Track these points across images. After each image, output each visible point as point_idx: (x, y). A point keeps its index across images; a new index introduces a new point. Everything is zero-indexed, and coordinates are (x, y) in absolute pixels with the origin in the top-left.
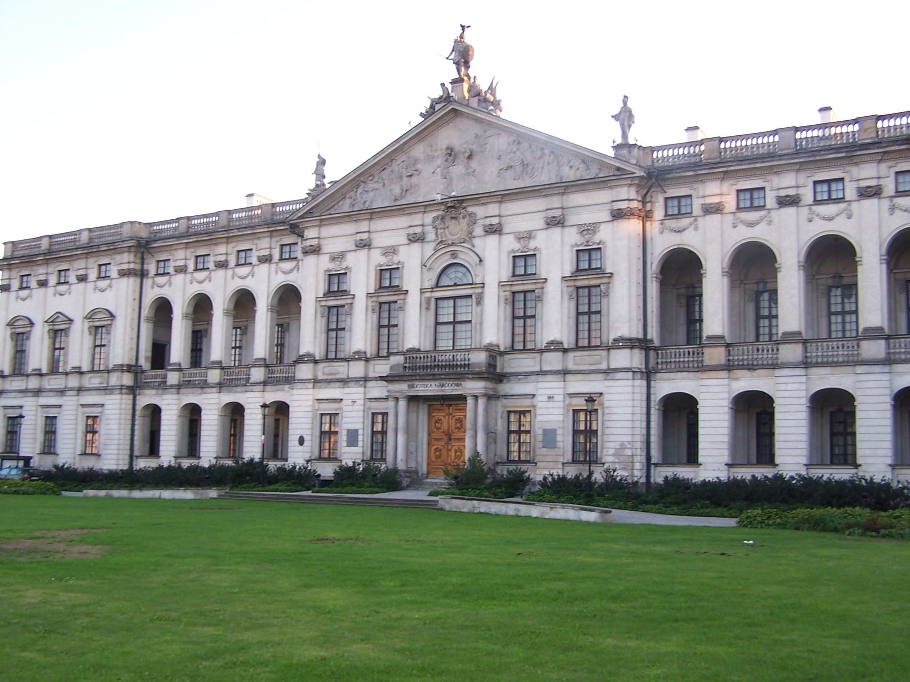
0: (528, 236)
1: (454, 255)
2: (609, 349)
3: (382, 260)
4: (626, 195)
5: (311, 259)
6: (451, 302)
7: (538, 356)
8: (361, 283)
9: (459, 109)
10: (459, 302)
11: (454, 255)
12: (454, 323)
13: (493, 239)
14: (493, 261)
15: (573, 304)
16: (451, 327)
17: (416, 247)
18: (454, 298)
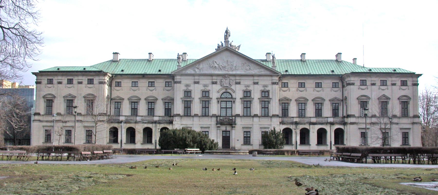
0: (248, 86)
1: (226, 89)
2: (271, 117)
3: (203, 88)
4: (276, 79)
5: (177, 86)
6: (225, 102)
7: (252, 119)
8: (197, 95)
9: (226, 49)
10: (227, 103)
11: (226, 89)
12: (226, 108)
13: (238, 86)
14: (238, 93)
15: (261, 105)
16: (225, 109)
17: (214, 86)
18: (226, 101)
